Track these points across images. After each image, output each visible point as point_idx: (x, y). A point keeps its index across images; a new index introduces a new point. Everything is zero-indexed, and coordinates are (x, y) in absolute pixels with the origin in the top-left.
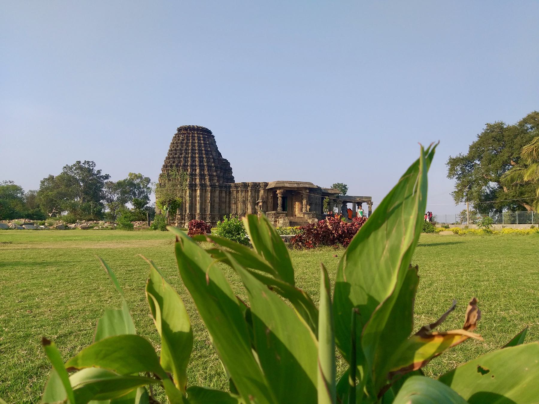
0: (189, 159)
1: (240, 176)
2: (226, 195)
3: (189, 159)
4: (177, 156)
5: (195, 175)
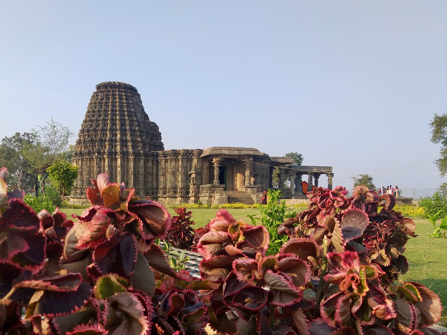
0: (109, 122)
1: (170, 142)
2: (153, 165)
3: (109, 122)
4: (94, 118)
5: (116, 141)
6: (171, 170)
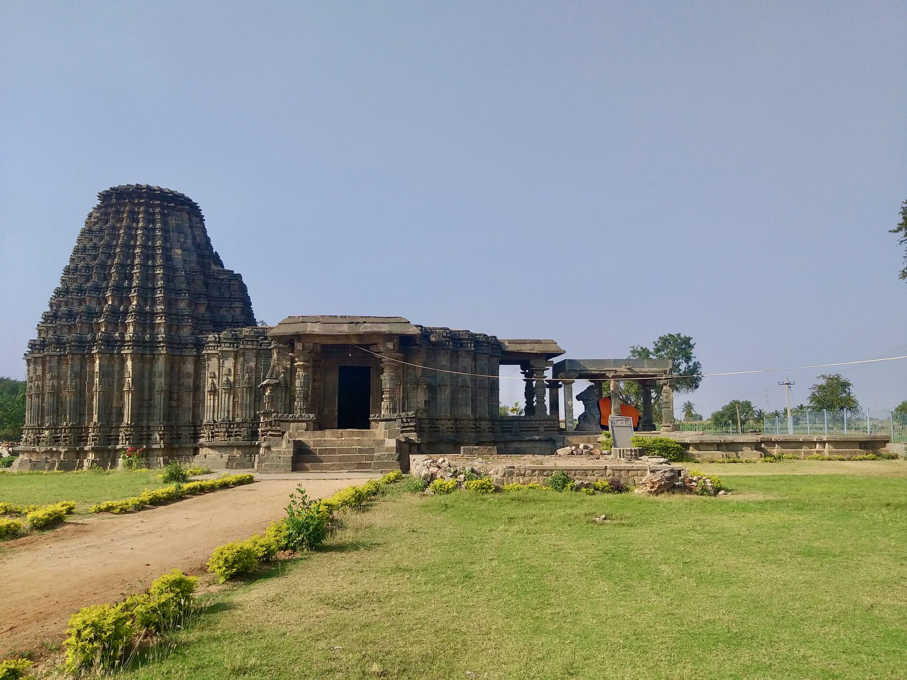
6: (225, 378)
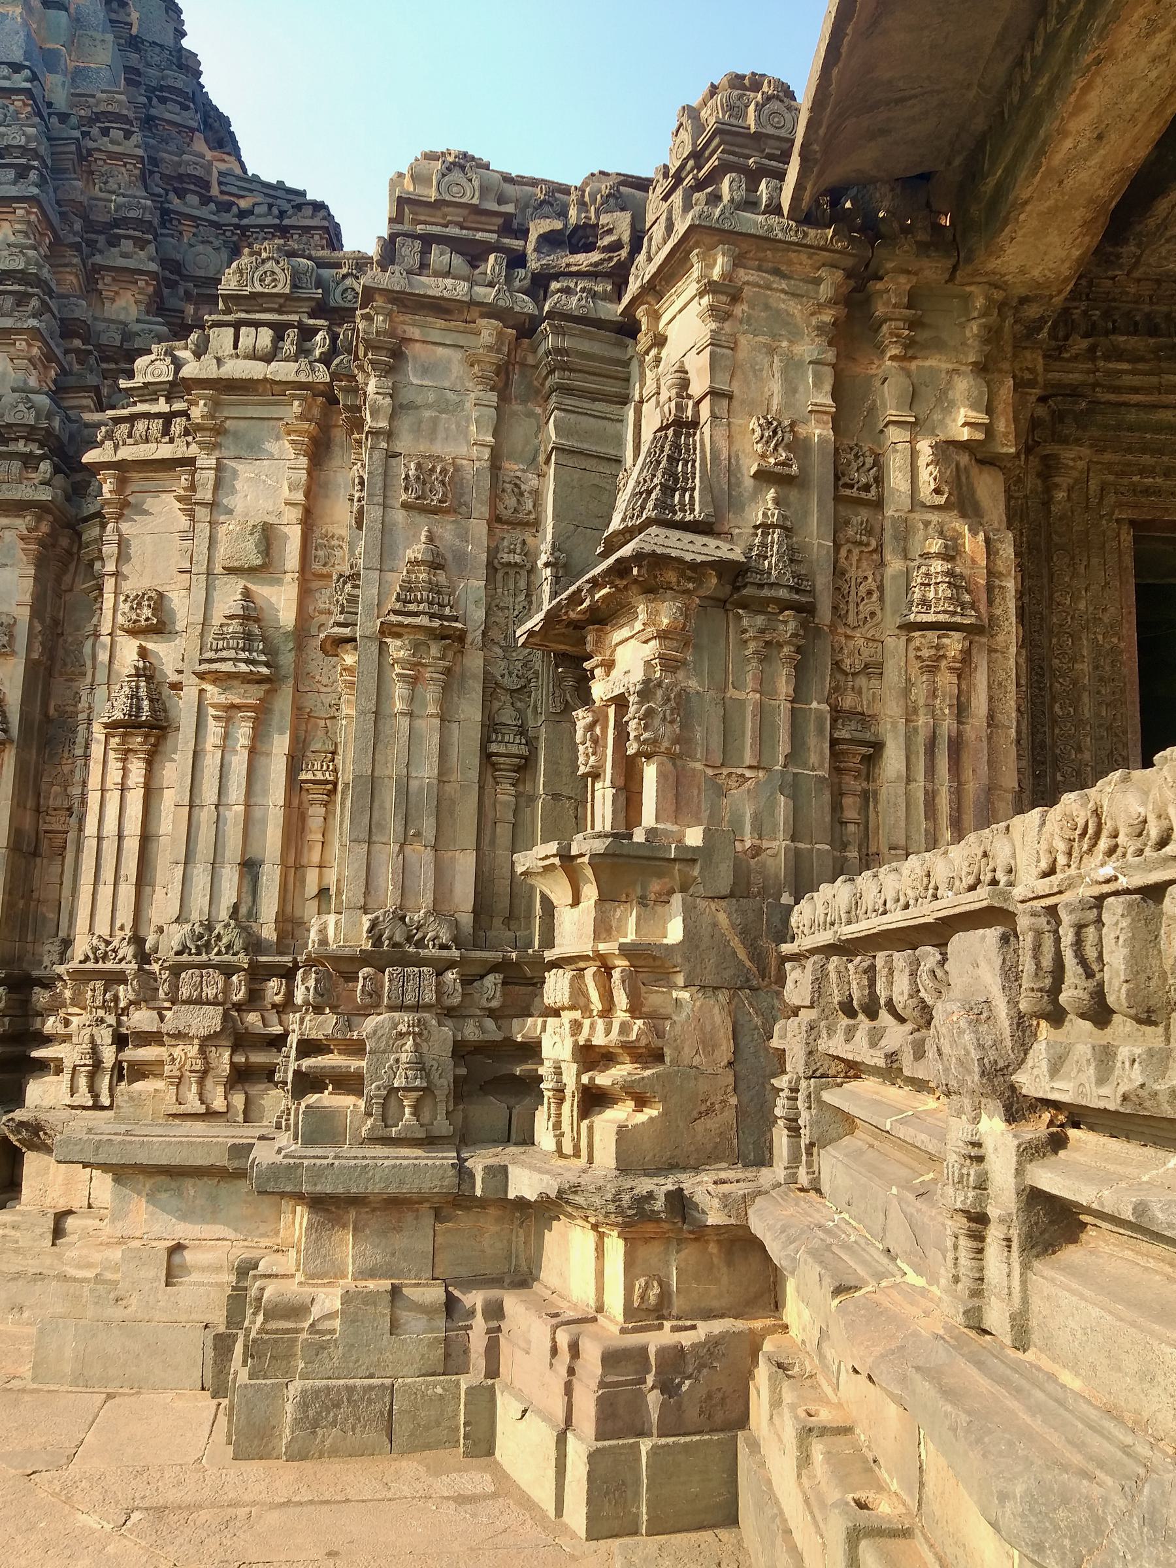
6: (229, 599)
